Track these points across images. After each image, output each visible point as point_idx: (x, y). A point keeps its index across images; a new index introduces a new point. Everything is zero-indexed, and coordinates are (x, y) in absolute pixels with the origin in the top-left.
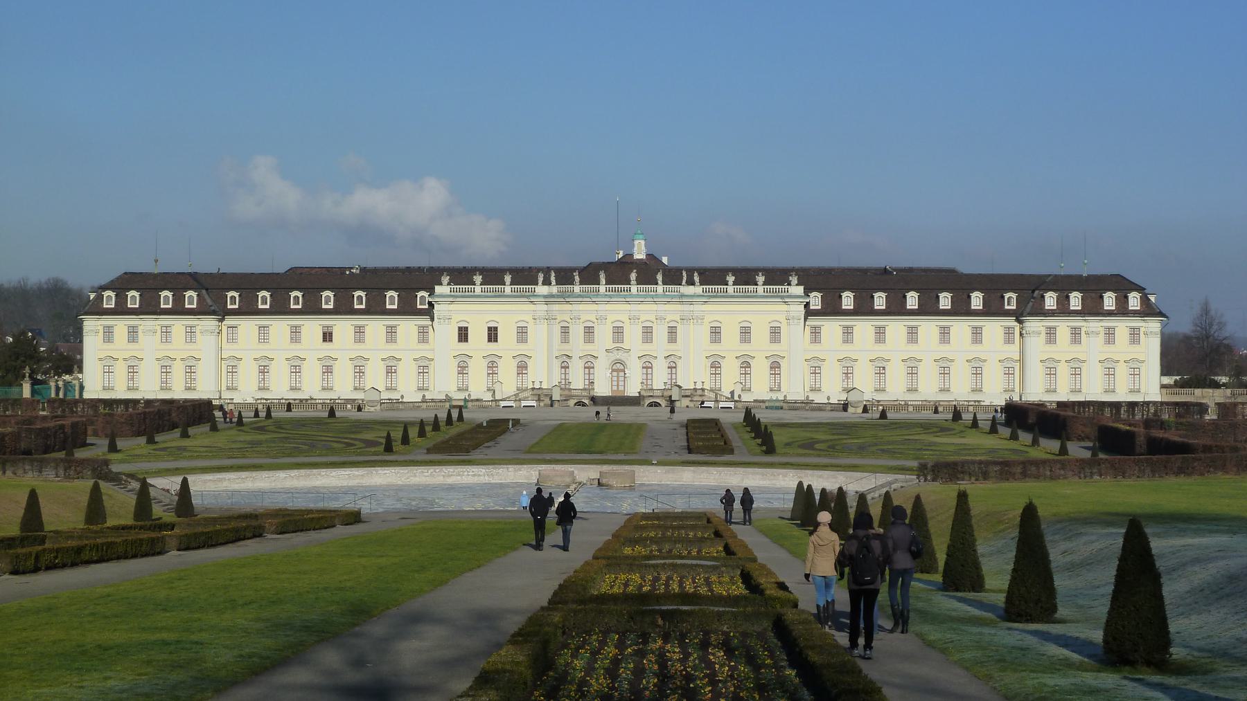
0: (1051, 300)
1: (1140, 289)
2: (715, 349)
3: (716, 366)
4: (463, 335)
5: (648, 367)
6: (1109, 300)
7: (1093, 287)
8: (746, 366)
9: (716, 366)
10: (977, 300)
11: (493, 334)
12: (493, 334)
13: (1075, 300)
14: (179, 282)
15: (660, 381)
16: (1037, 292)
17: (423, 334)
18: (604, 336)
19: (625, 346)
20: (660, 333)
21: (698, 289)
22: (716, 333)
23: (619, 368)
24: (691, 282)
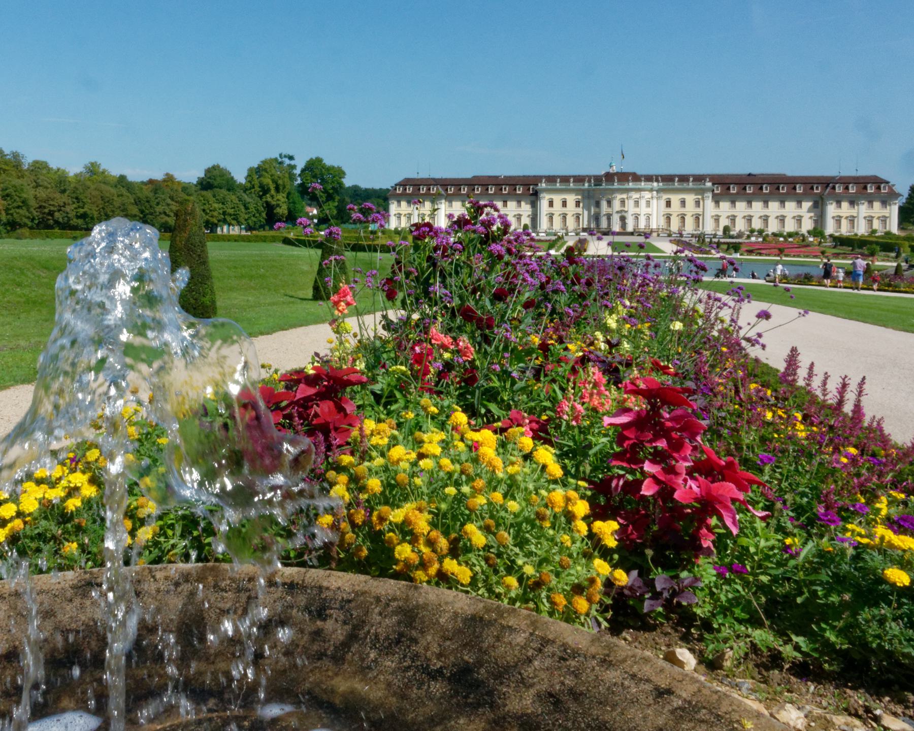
0: (839, 189)
1: (888, 183)
2: (668, 210)
3: (668, 218)
4: (551, 204)
5: (637, 218)
6: (871, 189)
7: (862, 183)
8: (683, 218)
9: (668, 218)
10: (800, 190)
11: (564, 204)
12: (564, 204)
13: (852, 190)
14: (430, 183)
15: (642, 225)
16: (831, 185)
17: (534, 205)
18: (617, 205)
19: (626, 209)
20: (643, 203)
21: (661, 184)
22: (668, 204)
23: (623, 219)
24: (657, 181)
